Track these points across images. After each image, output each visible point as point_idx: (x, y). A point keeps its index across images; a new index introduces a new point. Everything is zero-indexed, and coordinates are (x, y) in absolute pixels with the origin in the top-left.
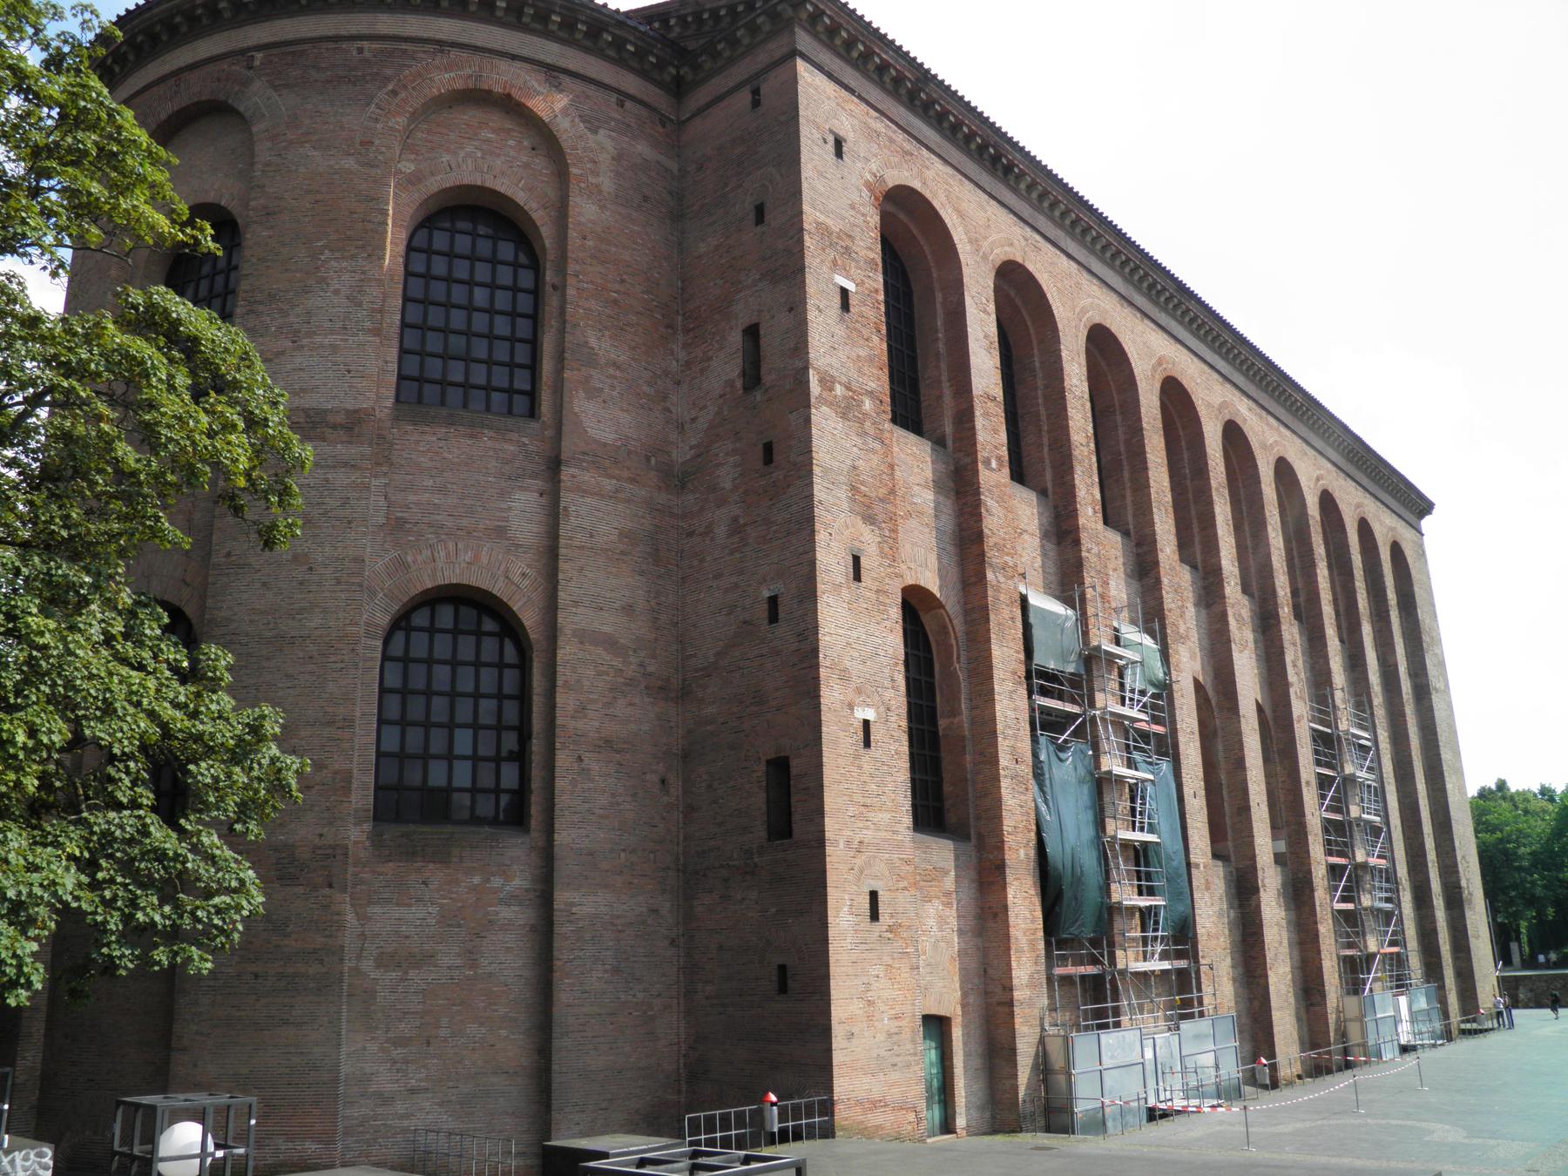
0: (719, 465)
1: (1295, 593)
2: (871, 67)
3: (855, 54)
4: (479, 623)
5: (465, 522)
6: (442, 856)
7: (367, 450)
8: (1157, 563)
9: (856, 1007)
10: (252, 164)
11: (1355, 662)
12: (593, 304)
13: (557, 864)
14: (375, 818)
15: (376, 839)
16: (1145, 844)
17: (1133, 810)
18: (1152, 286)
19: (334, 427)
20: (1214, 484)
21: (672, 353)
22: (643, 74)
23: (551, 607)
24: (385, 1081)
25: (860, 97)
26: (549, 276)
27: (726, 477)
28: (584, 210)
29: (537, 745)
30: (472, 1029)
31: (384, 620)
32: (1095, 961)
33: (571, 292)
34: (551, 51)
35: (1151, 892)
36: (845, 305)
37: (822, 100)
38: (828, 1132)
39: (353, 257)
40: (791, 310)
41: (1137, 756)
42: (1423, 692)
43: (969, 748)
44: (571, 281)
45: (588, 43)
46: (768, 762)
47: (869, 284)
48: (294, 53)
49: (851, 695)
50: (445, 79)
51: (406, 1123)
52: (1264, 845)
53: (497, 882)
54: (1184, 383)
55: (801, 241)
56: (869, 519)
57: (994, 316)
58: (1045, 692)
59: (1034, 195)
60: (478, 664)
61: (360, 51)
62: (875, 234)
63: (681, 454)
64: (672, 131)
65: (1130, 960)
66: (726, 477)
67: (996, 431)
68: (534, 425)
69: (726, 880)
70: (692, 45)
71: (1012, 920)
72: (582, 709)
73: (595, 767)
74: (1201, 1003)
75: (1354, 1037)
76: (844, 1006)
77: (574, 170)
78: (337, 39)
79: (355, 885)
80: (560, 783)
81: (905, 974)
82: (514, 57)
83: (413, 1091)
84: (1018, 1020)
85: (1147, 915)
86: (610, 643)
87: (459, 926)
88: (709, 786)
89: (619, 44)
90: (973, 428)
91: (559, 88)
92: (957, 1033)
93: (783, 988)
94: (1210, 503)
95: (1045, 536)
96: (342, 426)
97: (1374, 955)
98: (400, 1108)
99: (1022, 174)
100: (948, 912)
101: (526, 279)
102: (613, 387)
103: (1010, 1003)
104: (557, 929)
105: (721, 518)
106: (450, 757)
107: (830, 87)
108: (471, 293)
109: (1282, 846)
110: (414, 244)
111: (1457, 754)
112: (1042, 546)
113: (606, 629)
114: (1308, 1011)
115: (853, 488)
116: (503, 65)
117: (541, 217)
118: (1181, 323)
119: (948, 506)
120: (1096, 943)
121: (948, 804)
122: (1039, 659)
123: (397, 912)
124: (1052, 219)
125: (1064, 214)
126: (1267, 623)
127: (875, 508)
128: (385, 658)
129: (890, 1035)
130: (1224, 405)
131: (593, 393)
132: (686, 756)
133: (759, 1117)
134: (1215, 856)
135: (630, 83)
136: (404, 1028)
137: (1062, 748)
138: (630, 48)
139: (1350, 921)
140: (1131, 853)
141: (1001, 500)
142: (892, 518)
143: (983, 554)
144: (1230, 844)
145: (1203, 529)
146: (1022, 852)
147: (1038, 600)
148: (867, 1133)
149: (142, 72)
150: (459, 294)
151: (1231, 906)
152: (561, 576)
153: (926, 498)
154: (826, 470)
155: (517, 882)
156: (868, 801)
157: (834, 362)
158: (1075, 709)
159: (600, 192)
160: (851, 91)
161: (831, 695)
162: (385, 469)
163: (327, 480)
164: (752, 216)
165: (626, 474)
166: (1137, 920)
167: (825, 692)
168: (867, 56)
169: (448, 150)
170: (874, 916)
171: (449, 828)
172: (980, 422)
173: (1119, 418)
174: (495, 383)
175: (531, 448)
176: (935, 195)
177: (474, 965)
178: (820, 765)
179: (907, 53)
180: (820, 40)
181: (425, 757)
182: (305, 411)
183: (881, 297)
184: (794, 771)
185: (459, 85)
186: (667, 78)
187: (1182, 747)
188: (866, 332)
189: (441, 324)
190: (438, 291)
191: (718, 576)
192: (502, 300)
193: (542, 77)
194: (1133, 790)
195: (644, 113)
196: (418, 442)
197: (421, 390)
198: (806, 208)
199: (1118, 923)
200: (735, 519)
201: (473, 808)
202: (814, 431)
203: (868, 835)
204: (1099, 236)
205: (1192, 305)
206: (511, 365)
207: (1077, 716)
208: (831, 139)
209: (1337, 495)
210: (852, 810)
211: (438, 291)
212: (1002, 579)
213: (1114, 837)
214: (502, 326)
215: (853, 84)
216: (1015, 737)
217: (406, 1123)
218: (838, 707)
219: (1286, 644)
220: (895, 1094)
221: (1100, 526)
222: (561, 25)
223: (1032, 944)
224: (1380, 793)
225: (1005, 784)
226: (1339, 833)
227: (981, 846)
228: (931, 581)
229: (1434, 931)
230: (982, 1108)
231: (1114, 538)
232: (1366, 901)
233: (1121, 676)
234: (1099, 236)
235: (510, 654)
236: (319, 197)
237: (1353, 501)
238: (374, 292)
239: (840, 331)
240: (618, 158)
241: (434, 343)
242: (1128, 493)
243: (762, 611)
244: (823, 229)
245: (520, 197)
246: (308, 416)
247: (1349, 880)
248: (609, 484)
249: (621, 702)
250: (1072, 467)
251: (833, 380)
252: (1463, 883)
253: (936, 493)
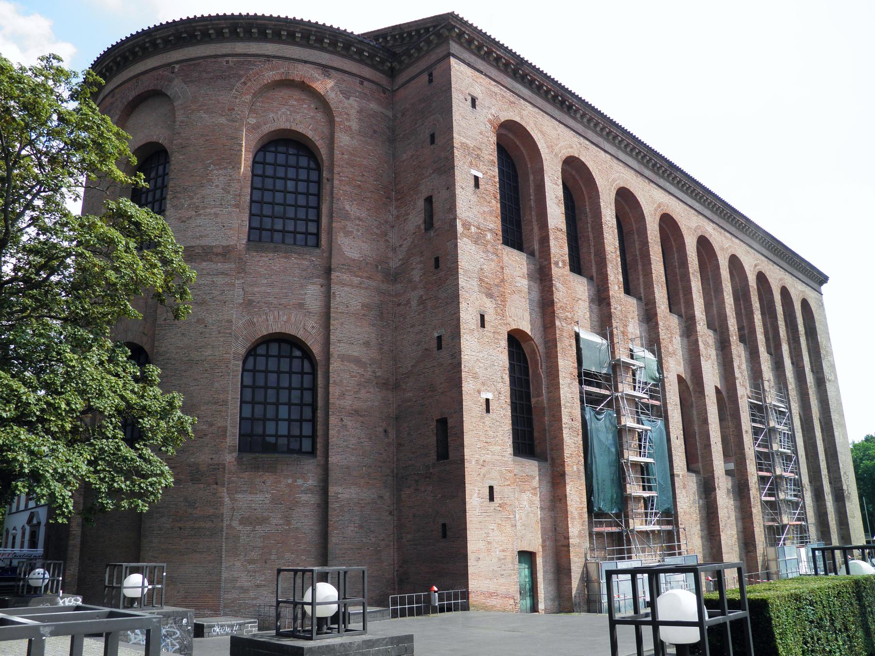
0: (413, 269)
1: (741, 329)
2: (491, 59)
3: (482, 53)
4: (291, 352)
5: (283, 301)
6: (272, 469)
7: (233, 266)
8: (656, 314)
9: (481, 545)
10: (174, 122)
11: (778, 366)
12: (347, 188)
13: (330, 473)
14: (239, 450)
15: (239, 460)
16: (647, 464)
17: (640, 446)
18: (654, 165)
19: (217, 255)
20: (691, 270)
21: (389, 211)
22: (373, 66)
23: (327, 343)
24: (244, 581)
25: (486, 75)
26: (325, 174)
27: (416, 275)
28: (343, 140)
29: (320, 413)
30: (287, 555)
31: (242, 351)
32: (618, 525)
33: (336, 182)
34: (325, 58)
35: (650, 489)
36: (477, 185)
37: (464, 78)
38: (466, 607)
39: (225, 168)
40: (448, 189)
41: (643, 417)
42: (821, 382)
43: (547, 413)
44: (336, 177)
45: (344, 53)
46: (437, 421)
47: (490, 173)
48: (195, 65)
49: (479, 386)
50: (270, 75)
51: (255, 602)
52: (719, 464)
53: (300, 482)
54: (674, 216)
55: (453, 153)
56: (490, 295)
57: (561, 186)
58: (589, 384)
59: (585, 120)
60: (290, 373)
61: (227, 62)
62: (494, 147)
63: (394, 263)
64: (389, 95)
65: (637, 525)
66: (416, 275)
67: (562, 247)
68: (318, 251)
69: (417, 481)
70: (398, 50)
71: (569, 502)
72: (342, 395)
73: (349, 423)
74: (679, 548)
75: (773, 569)
76: (475, 544)
77: (337, 119)
78: (216, 56)
79: (229, 484)
80: (331, 432)
81: (508, 529)
82: (306, 62)
83: (258, 586)
84: (572, 554)
85: (647, 501)
86: (357, 361)
87: (281, 504)
88: (409, 433)
89: (360, 52)
90: (549, 246)
91: (329, 76)
92: (539, 561)
93: (444, 536)
94: (689, 281)
95: (592, 301)
96: (221, 254)
97: (786, 525)
98: (252, 594)
99: (577, 110)
100: (534, 498)
101: (314, 176)
102: (358, 230)
103: (568, 546)
104: (330, 506)
105: (414, 296)
106: (277, 420)
107: (469, 71)
108: (286, 184)
109: (732, 466)
110: (256, 160)
111: (842, 415)
112: (590, 307)
113: (356, 354)
114: (747, 556)
115: (481, 280)
116: (300, 66)
117: (321, 145)
118: (672, 184)
119: (536, 287)
120: (618, 516)
121: (536, 443)
122: (586, 366)
123: (250, 497)
124: (596, 132)
125: (602, 129)
126: (723, 346)
127: (493, 290)
128: (244, 370)
129: (500, 560)
130: (698, 227)
131: (348, 234)
132: (397, 418)
133: (428, 599)
134: (689, 470)
135: (366, 71)
136: (254, 555)
137: (599, 413)
138: (366, 54)
139: (773, 508)
140: (639, 469)
141: (564, 283)
142: (503, 295)
143: (554, 312)
144: (700, 465)
145: (685, 295)
146: (575, 467)
147: (585, 335)
148: (486, 608)
149: (120, 75)
150: (279, 184)
151: (700, 498)
152: (331, 327)
153: (523, 283)
154: (466, 271)
155: (310, 482)
156: (489, 440)
157: (470, 214)
158: (607, 393)
159: (351, 130)
160: (481, 72)
161: (468, 386)
162: (243, 275)
163: (213, 281)
164: (429, 139)
165: (365, 275)
166: (642, 504)
167: (464, 384)
168: (489, 53)
169: (272, 112)
170: (492, 498)
171: (276, 455)
172: (552, 243)
173: (636, 237)
174: (298, 230)
175: (316, 263)
176: (528, 124)
177: (288, 523)
178: (462, 422)
179: (511, 50)
180: (464, 47)
181: (264, 420)
182: (202, 246)
183: (497, 180)
184: (449, 425)
185: (277, 78)
186: (386, 68)
187: (670, 413)
188: (488, 199)
189: (270, 200)
190: (269, 183)
191: (412, 327)
192: (302, 187)
193: (320, 72)
194: (640, 435)
195: (374, 87)
196: (259, 261)
197: (261, 235)
198: (455, 135)
199: (631, 505)
200: (421, 297)
201: (288, 445)
202: (459, 251)
203: (488, 458)
204: (623, 140)
205: (678, 174)
206: (307, 220)
207: (608, 396)
208: (469, 98)
209: (767, 274)
210: (479, 445)
211: (269, 183)
212: (565, 325)
213: (628, 460)
214: (302, 201)
215: (482, 68)
216: (572, 407)
217: (255, 602)
218: (472, 392)
219: (734, 356)
220: (502, 590)
221: (622, 295)
222: (329, 44)
223: (581, 515)
224: (792, 438)
225: (565, 432)
226: (765, 460)
227: (553, 464)
228: (527, 328)
229: (826, 514)
230: (553, 600)
231: (632, 302)
232: (782, 496)
233: (634, 375)
234: (623, 140)
235: (307, 367)
236: (208, 138)
237: (777, 277)
238: (236, 185)
239: (474, 199)
240: (360, 112)
241: (267, 210)
242: (641, 277)
243: (434, 344)
244: (464, 146)
245: (310, 134)
246: (203, 249)
247: (772, 485)
248: (356, 280)
249: (363, 391)
250: (606, 265)
251: (470, 224)
252: (845, 487)
253: (529, 281)
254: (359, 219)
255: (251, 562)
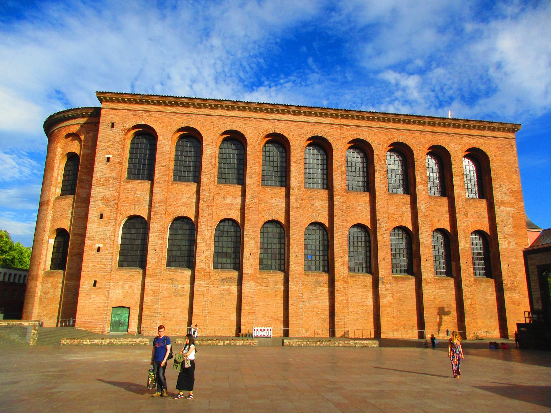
115: (103, 200)
154: (95, 199)
160: (121, 109)
161: (88, 243)
177: (54, 294)
251: (101, 178)
254: (88, 181)
255: (44, 307)
